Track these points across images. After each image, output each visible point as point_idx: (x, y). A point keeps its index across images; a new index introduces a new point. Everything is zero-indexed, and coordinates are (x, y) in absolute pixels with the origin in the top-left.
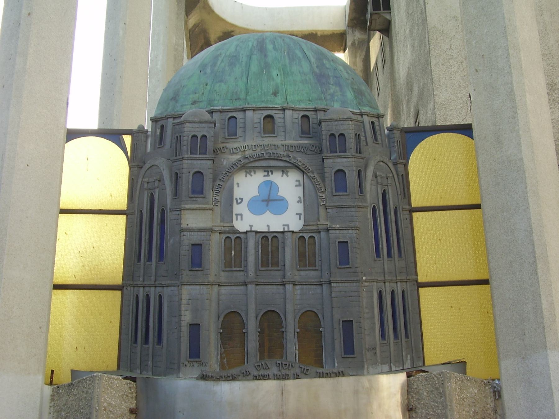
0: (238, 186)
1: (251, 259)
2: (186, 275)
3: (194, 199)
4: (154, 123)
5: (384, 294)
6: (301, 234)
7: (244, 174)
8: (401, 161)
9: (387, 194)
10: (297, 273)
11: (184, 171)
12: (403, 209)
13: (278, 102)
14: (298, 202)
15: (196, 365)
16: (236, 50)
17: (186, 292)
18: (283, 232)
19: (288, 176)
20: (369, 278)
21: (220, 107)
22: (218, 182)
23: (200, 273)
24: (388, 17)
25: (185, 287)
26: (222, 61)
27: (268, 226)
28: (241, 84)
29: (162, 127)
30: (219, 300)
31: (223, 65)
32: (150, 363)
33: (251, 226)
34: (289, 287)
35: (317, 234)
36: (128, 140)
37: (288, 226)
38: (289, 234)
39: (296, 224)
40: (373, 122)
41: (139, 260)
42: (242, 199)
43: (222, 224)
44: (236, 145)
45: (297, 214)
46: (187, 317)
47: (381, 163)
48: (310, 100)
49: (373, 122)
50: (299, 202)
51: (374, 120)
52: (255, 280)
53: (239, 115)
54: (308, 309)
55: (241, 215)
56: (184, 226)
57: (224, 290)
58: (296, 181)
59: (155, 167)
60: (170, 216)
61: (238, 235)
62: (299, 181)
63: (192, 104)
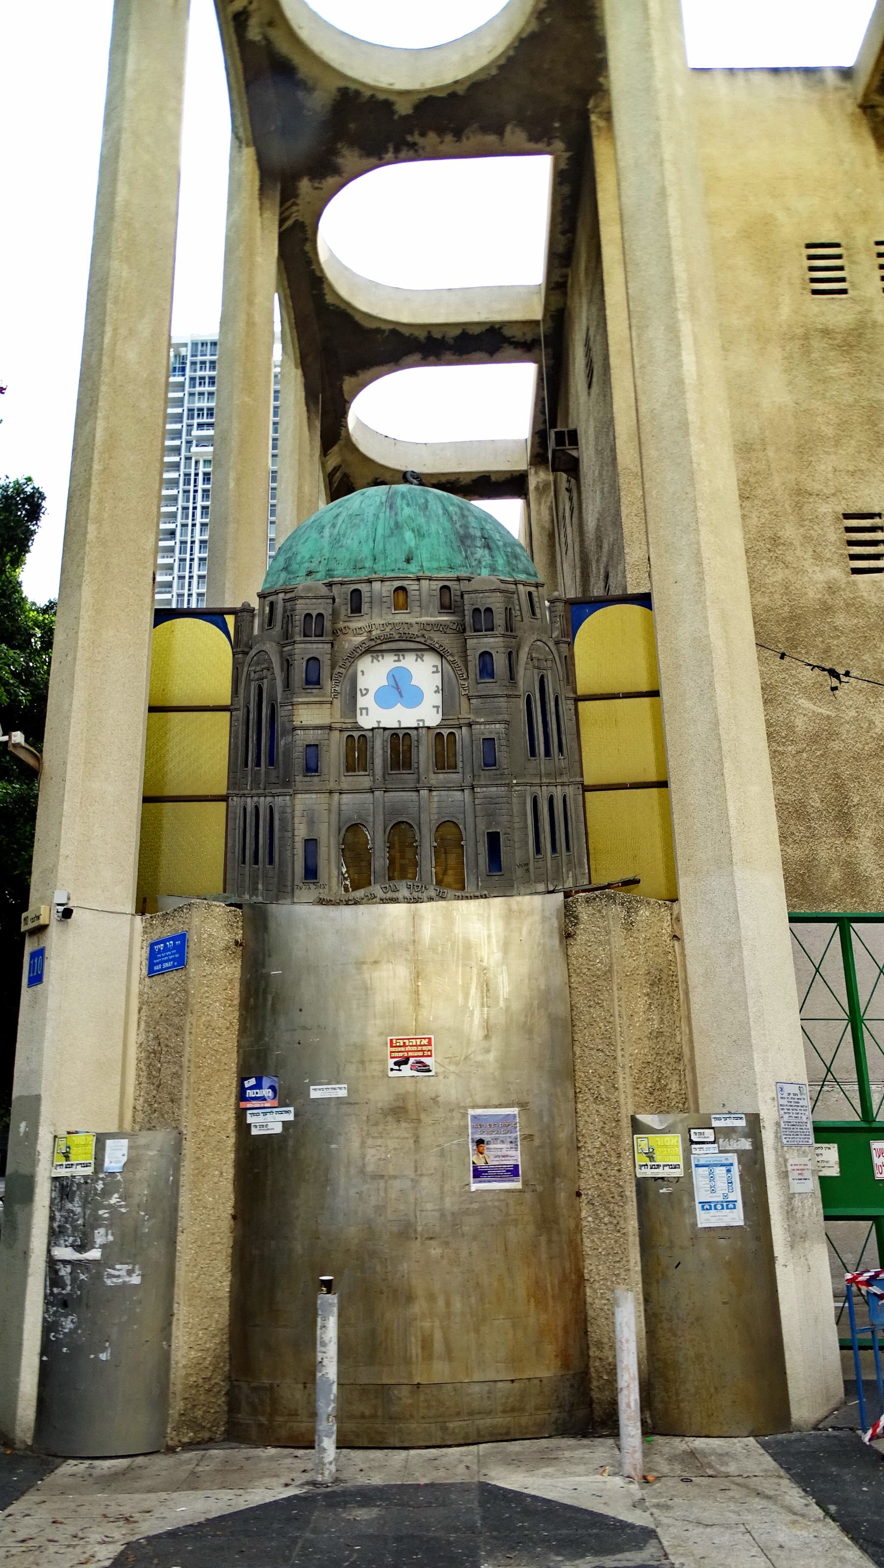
0: (363, 674)
1: (378, 761)
3: (309, 691)
4: (262, 599)
5: (540, 800)
6: (438, 731)
7: (370, 659)
8: (564, 639)
9: (546, 680)
10: (432, 776)
11: (296, 657)
12: (567, 698)
14: (435, 692)
15: (312, 886)
16: (360, 507)
17: (303, 801)
18: (416, 728)
19: (423, 661)
20: (520, 781)
21: (340, 579)
22: (337, 670)
23: (316, 779)
24: (574, 453)
25: (299, 796)
26: (343, 522)
27: (399, 722)
28: (366, 551)
29: (272, 604)
30: (340, 810)
31: (344, 525)
32: (260, 886)
33: (379, 722)
34: (424, 793)
35: (459, 730)
37: (423, 721)
38: (424, 731)
39: (433, 719)
40: (530, 593)
41: (246, 765)
42: (367, 690)
43: (342, 720)
44: (360, 625)
45: (434, 707)
46: (301, 832)
47: (539, 643)
48: (451, 568)
49: (530, 593)
50: (437, 692)
51: (532, 589)
52: (383, 786)
53: (363, 587)
54: (447, 819)
55: (367, 709)
56: (296, 723)
57: (345, 798)
58: (434, 666)
59: (262, 653)
60: (282, 712)
61: (362, 733)
62: (436, 666)
63: (307, 575)
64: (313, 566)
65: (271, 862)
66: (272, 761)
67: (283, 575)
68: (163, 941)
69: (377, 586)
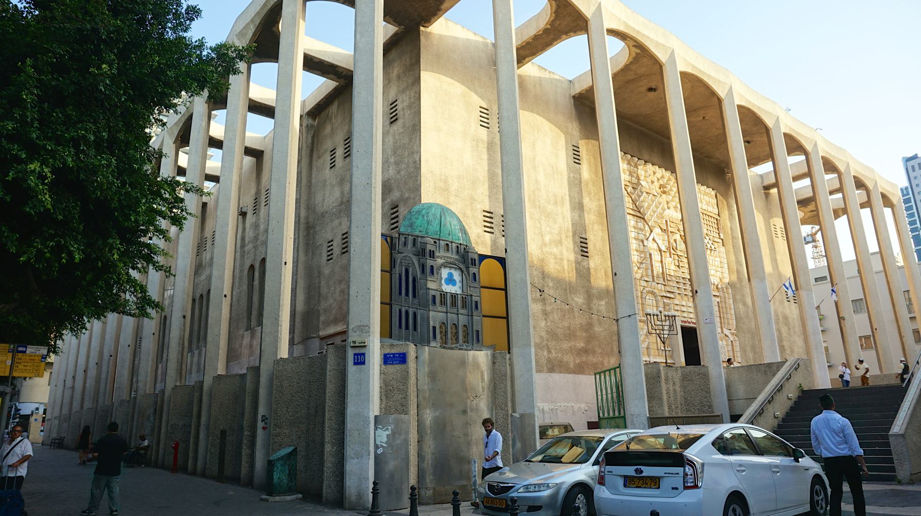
2: (431, 307)
13: (450, 239)
36: (389, 239)
39: (459, 292)
60: (420, 282)
64: (421, 229)
65: (415, 329)
66: (414, 296)
67: (409, 228)
68: (394, 354)
69: (441, 241)
